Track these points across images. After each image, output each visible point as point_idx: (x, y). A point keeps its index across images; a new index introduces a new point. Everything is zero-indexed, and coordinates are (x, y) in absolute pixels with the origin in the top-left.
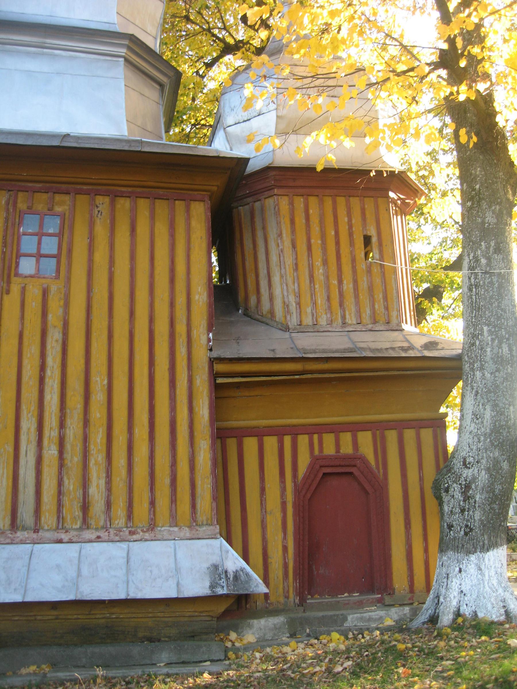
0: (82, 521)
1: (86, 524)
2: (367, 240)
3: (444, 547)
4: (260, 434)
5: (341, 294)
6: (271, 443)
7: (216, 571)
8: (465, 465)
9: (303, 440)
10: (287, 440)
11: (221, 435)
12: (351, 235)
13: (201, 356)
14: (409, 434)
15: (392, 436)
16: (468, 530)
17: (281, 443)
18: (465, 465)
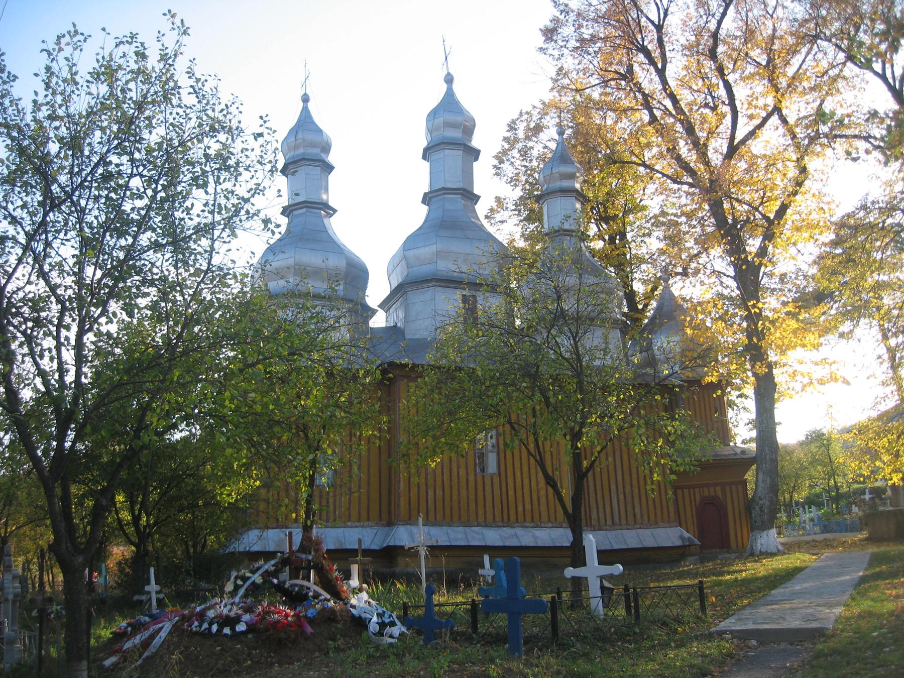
0: (633, 522)
3: (752, 530)
4: (682, 488)
6: (686, 491)
7: (682, 537)
8: (760, 499)
9: (697, 490)
15: (727, 488)
16: (763, 522)
18: (760, 499)
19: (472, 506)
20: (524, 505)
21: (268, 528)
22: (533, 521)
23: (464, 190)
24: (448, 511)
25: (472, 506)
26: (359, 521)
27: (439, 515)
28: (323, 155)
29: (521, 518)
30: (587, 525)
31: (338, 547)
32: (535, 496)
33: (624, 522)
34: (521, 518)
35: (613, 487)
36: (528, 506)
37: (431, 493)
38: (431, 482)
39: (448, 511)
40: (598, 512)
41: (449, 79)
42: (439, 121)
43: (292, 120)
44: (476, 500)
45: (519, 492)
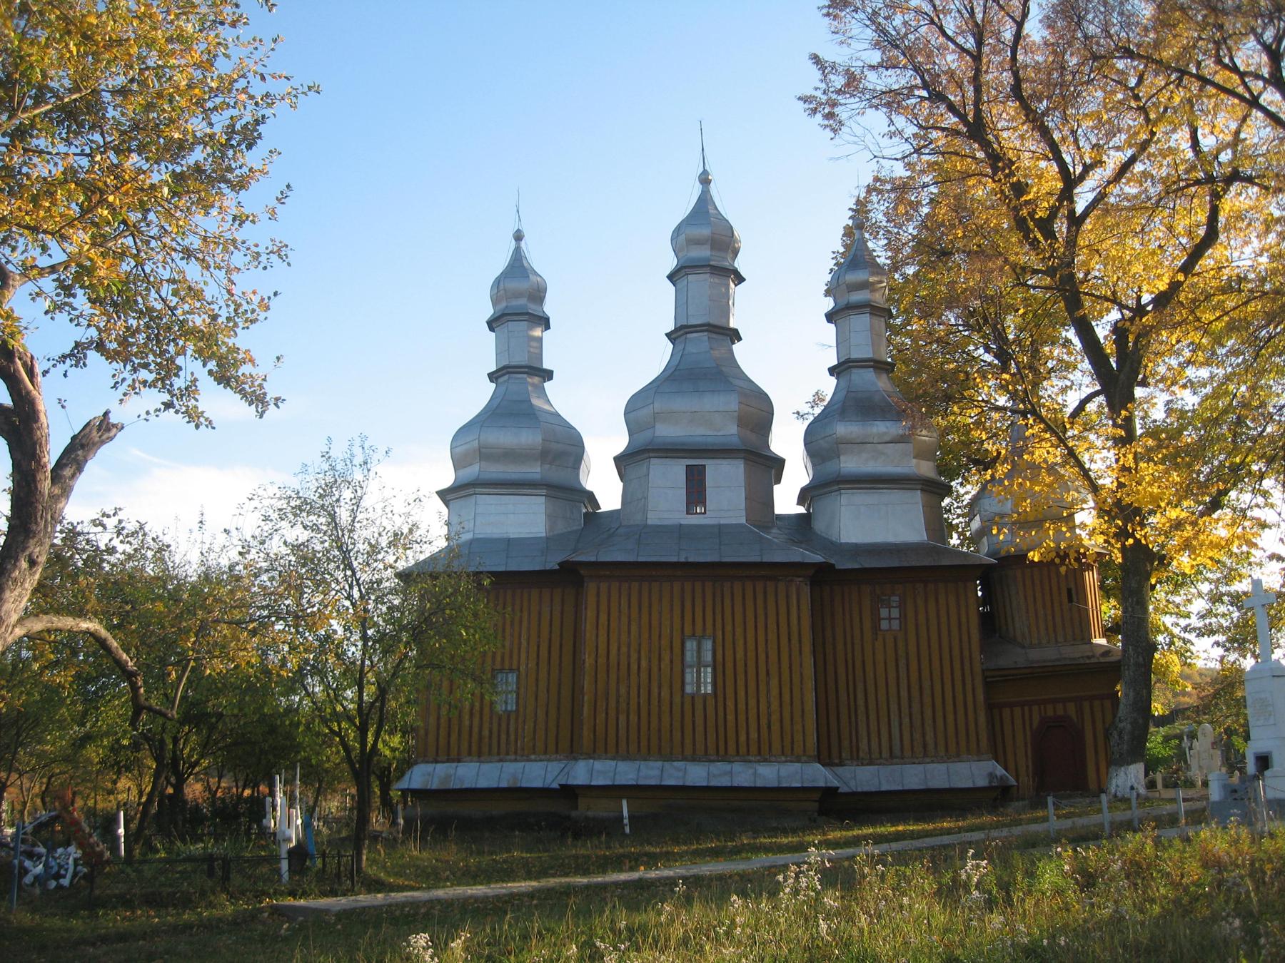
0: (923, 753)
1: (925, 755)
2: (1069, 591)
3: (1110, 763)
5: (1054, 626)
6: (1018, 710)
7: (991, 776)
9: (1035, 708)
10: (1026, 708)
11: (991, 707)
12: (1059, 588)
13: (978, 668)
14: (1097, 703)
15: (1086, 705)
16: (1121, 755)
17: (1023, 710)
19: (677, 735)
20: (748, 734)
21: (437, 762)
22: (759, 753)
23: (708, 325)
24: (644, 743)
25: (677, 735)
26: (545, 753)
27: (633, 747)
28: (532, 308)
29: (743, 750)
30: (852, 759)
31: (511, 785)
32: (764, 721)
33: (908, 753)
34: (743, 750)
35: (894, 707)
36: (754, 735)
37: (622, 718)
38: (623, 706)
39: (644, 743)
40: (869, 740)
41: (705, 180)
42: (683, 237)
43: (500, 262)
44: (682, 727)
45: (742, 717)
